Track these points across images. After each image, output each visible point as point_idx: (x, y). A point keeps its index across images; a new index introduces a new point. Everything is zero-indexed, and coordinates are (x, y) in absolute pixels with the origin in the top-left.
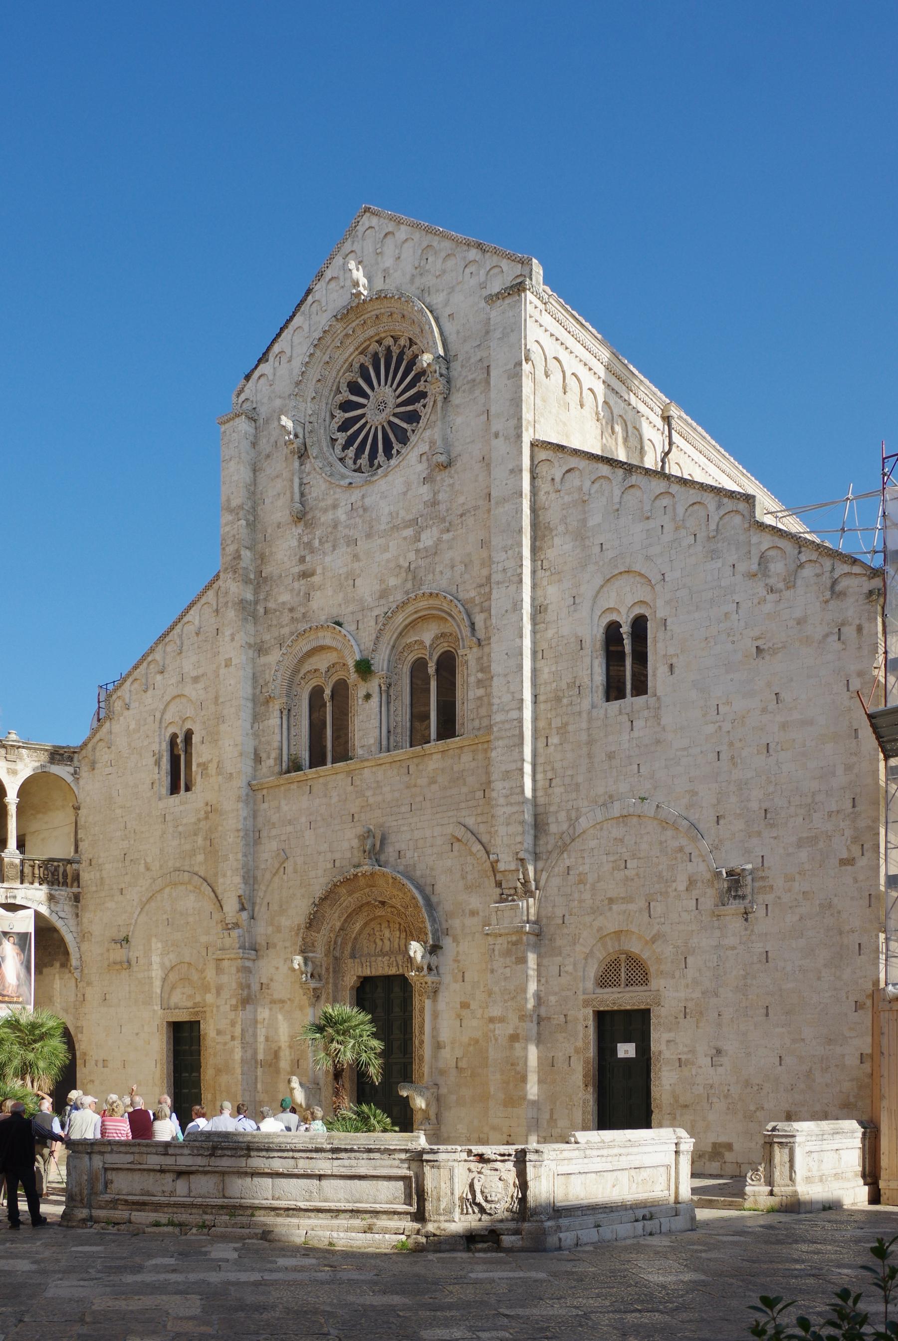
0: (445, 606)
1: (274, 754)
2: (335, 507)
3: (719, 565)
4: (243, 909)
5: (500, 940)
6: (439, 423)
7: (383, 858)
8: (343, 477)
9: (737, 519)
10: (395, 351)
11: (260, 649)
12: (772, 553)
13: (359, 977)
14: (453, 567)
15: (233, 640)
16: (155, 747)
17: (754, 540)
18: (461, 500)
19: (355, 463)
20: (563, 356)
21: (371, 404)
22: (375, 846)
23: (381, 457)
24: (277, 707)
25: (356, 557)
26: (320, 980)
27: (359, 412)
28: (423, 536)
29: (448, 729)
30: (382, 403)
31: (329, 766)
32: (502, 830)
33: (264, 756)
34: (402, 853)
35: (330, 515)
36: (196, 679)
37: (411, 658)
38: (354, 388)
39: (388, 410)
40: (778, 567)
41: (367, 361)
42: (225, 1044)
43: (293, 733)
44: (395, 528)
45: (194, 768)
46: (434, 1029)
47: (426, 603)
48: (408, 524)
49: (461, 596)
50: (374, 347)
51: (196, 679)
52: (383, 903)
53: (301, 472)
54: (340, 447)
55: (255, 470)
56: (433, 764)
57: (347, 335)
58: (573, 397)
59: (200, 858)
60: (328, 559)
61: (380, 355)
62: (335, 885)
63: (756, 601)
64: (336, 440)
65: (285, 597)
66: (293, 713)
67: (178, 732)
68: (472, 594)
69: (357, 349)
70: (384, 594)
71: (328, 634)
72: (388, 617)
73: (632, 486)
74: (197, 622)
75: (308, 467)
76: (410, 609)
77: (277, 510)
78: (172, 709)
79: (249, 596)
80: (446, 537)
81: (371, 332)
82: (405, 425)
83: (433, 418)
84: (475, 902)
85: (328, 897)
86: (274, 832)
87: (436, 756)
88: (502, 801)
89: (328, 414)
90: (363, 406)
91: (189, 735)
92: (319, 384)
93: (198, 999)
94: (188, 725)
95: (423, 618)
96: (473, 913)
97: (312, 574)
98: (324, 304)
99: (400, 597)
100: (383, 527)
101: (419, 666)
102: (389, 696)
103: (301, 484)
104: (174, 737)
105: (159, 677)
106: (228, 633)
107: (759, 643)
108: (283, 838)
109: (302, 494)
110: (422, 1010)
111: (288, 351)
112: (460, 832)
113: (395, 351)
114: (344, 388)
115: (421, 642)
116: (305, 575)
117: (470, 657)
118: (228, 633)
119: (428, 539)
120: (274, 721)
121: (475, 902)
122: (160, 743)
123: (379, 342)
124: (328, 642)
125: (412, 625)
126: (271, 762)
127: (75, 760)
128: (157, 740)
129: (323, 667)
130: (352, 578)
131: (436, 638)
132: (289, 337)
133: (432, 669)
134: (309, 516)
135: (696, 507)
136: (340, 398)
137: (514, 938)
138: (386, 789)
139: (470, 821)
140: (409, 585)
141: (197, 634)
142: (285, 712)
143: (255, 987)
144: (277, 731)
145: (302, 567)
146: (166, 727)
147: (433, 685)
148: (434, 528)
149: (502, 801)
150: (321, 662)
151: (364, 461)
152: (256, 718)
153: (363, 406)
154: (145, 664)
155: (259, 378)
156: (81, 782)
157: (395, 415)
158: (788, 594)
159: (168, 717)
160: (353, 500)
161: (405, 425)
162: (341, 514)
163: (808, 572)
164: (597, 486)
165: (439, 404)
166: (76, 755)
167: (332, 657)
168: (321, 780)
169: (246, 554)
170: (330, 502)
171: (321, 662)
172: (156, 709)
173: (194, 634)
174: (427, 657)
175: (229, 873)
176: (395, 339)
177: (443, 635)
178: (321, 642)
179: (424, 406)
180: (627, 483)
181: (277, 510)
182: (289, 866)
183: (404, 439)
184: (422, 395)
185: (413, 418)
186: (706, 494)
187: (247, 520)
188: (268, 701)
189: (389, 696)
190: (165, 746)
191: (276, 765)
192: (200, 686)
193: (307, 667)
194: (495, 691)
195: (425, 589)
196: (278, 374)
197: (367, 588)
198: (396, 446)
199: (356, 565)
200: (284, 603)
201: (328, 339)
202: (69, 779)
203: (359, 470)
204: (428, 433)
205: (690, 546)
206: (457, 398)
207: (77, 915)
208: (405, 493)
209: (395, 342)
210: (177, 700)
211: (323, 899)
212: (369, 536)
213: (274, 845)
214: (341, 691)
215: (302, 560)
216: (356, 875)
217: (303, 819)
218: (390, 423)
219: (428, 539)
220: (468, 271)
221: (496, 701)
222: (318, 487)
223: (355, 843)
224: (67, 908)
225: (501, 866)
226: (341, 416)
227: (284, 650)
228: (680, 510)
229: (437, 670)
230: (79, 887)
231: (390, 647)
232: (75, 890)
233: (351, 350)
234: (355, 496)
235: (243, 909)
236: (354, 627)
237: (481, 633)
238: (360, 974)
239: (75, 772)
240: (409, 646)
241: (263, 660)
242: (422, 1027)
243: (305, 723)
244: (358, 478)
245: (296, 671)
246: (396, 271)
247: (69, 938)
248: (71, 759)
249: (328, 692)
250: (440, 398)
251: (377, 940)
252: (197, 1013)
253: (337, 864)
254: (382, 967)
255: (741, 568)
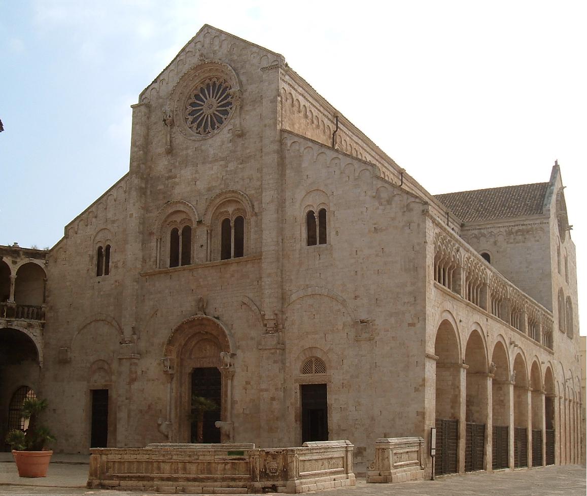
0: (240, 197)
1: (152, 260)
2: (187, 148)
3: (359, 191)
4: (134, 333)
5: (266, 352)
6: (238, 117)
7: (207, 311)
8: (192, 136)
9: (368, 173)
10: (218, 84)
11: (146, 209)
12: (382, 189)
13: (193, 368)
14: (243, 180)
15: (134, 205)
16: (90, 253)
17: (374, 183)
18: (248, 151)
19: (197, 129)
20: (293, 92)
21: (205, 106)
22: (202, 305)
23: (209, 129)
24: (155, 237)
25: (197, 172)
26: (173, 369)
27: (200, 108)
28: (230, 165)
29: (239, 252)
30: (211, 105)
31: (180, 266)
32: (267, 300)
33: (148, 261)
34: (217, 309)
35: (185, 152)
36: (113, 222)
37: (223, 218)
38: (197, 97)
39: (213, 108)
40: (384, 195)
41: (204, 87)
42: (122, 401)
43: (162, 250)
44: (216, 161)
45: (110, 264)
46: (232, 394)
47: (230, 194)
48: (223, 159)
49: (247, 193)
50: (207, 81)
51: (113, 222)
52: (207, 333)
53: (171, 132)
54: (190, 122)
55: (148, 129)
56: (233, 268)
57: (196, 76)
58: (295, 109)
59: (112, 308)
60: (182, 172)
61: (210, 85)
62: (183, 323)
63: (375, 208)
64: (188, 119)
65: (161, 187)
66: (163, 240)
67: (102, 246)
68: (253, 192)
69: (200, 81)
70: (209, 190)
71: (182, 205)
72: (212, 201)
73: (322, 153)
74: (115, 195)
75: (174, 130)
76: (223, 197)
77: (158, 148)
78: (100, 235)
79: (143, 186)
80: (240, 166)
81: (207, 75)
82: (221, 116)
83: (235, 115)
84: (253, 333)
85: (179, 329)
86: (152, 296)
87: (234, 266)
88: (267, 287)
89: (184, 108)
90: (203, 105)
91: (108, 247)
92: (181, 95)
93: (107, 378)
94: (108, 243)
95: (229, 201)
96: (252, 339)
97: (175, 177)
98: (184, 61)
99: (218, 191)
100: (210, 160)
101: (226, 223)
102: (211, 235)
103: (170, 137)
104: (100, 248)
105: (94, 220)
106: (132, 201)
107: (376, 226)
108: (156, 299)
109: (171, 142)
110: (226, 386)
111: (166, 79)
112: (246, 300)
113: (218, 84)
114: (193, 97)
115: (227, 212)
116: (169, 178)
117: (252, 220)
118: (132, 201)
119: (232, 166)
120: (154, 244)
121: (253, 333)
122: (93, 251)
123: (210, 79)
124: (182, 209)
125: (223, 204)
126: (151, 263)
127: (47, 257)
128: (91, 249)
129: (178, 221)
130: (195, 181)
131: (235, 210)
132: (167, 73)
133: (232, 224)
134: (174, 152)
135: (350, 165)
136: (190, 101)
137: (273, 351)
138: (209, 279)
139: (251, 295)
140: (222, 186)
141: (115, 201)
142: (159, 240)
143: (139, 373)
144: (155, 248)
145: (170, 174)
146: (96, 244)
147: (233, 231)
148: (235, 162)
149: (267, 287)
150: (178, 218)
151: (201, 129)
152: (143, 243)
153: (203, 105)
154: (87, 213)
155: (152, 89)
156: (49, 268)
157: (217, 111)
158: (388, 207)
159: (98, 239)
160: (196, 146)
161: (221, 116)
162: (190, 152)
163: (397, 198)
164: (306, 150)
165: (238, 110)
166: (47, 255)
167: (184, 216)
168: (176, 273)
169: (143, 166)
170: (184, 146)
171: (178, 218)
172: (92, 235)
173: (113, 200)
174: (230, 219)
175: (128, 316)
176: (218, 79)
177: (238, 209)
178: (178, 209)
179: (231, 108)
180: (320, 151)
181: (158, 148)
182: (159, 314)
183: (221, 122)
184: (230, 103)
185: (226, 113)
186: (354, 161)
187: (144, 151)
188: (151, 234)
189: (211, 235)
190: (95, 253)
191: (153, 264)
192: (115, 225)
193: (170, 220)
194: (264, 237)
195: (230, 188)
196: (161, 88)
197: (201, 186)
198: (217, 125)
199: (197, 175)
200: (160, 189)
201: (187, 76)
202: (43, 266)
203: (199, 133)
204: (232, 121)
205: (346, 181)
206: (247, 108)
207: (43, 334)
208: (221, 146)
209: (218, 80)
210: (103, 231)
211: (177, 330)
212: (203, 163)
213: (152, 303)
214: (187, 231)
215: (171, 171)
216: (194, 319)
217: (167, 291)
218: (214, 114)
219: (232, 166)
220: (252, 56)
221: (265, 241)
222: (179, 139)
223: (193, 303)
224: (38, 331)
225: (267, 317)
226: (190, 108)
227: (160, 211)
228: (343, 166)
229: (235, 226)
230: (44, 320)
231: (212, 213)
232: (42, 321)
233: (197, 81)
234: (197, 144)
235: (134, 333)
236: (195, 203)
237: (256, 210)
238: (195, 367)
239: (46, 263)
240: (221, 213)
241: (149, 215)
242: (226, 391)
243: (168, 245)
244: (198, 137)
245: (165, 221)
246: (219, 52)
247: (39, 346)
248: (44, 256)
249: (180, 232)
250: (238, 107)
251: (203, 350)
252: (106, 386)
253: (184, 313)
254: (206, 364)
255: (369, 193)
